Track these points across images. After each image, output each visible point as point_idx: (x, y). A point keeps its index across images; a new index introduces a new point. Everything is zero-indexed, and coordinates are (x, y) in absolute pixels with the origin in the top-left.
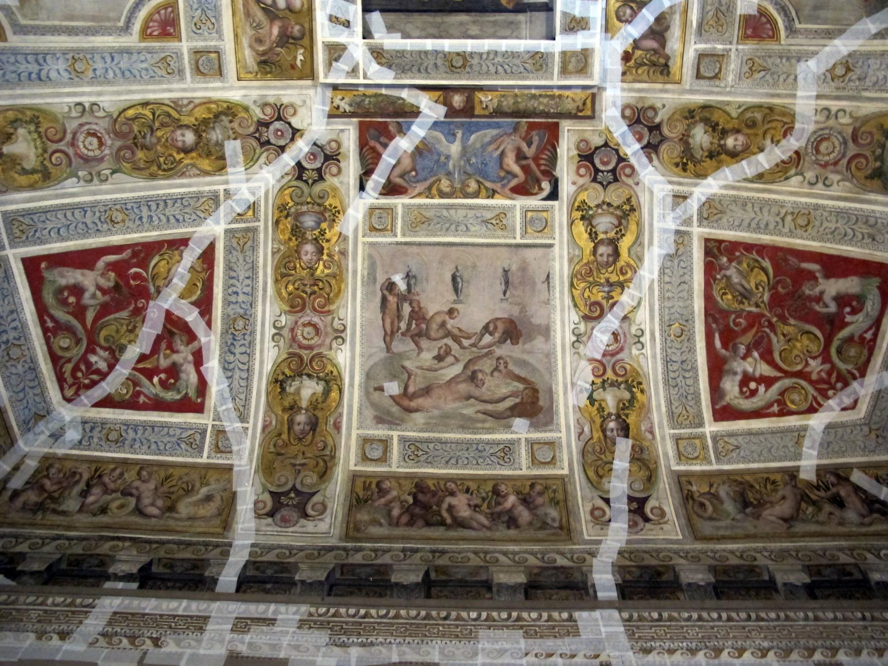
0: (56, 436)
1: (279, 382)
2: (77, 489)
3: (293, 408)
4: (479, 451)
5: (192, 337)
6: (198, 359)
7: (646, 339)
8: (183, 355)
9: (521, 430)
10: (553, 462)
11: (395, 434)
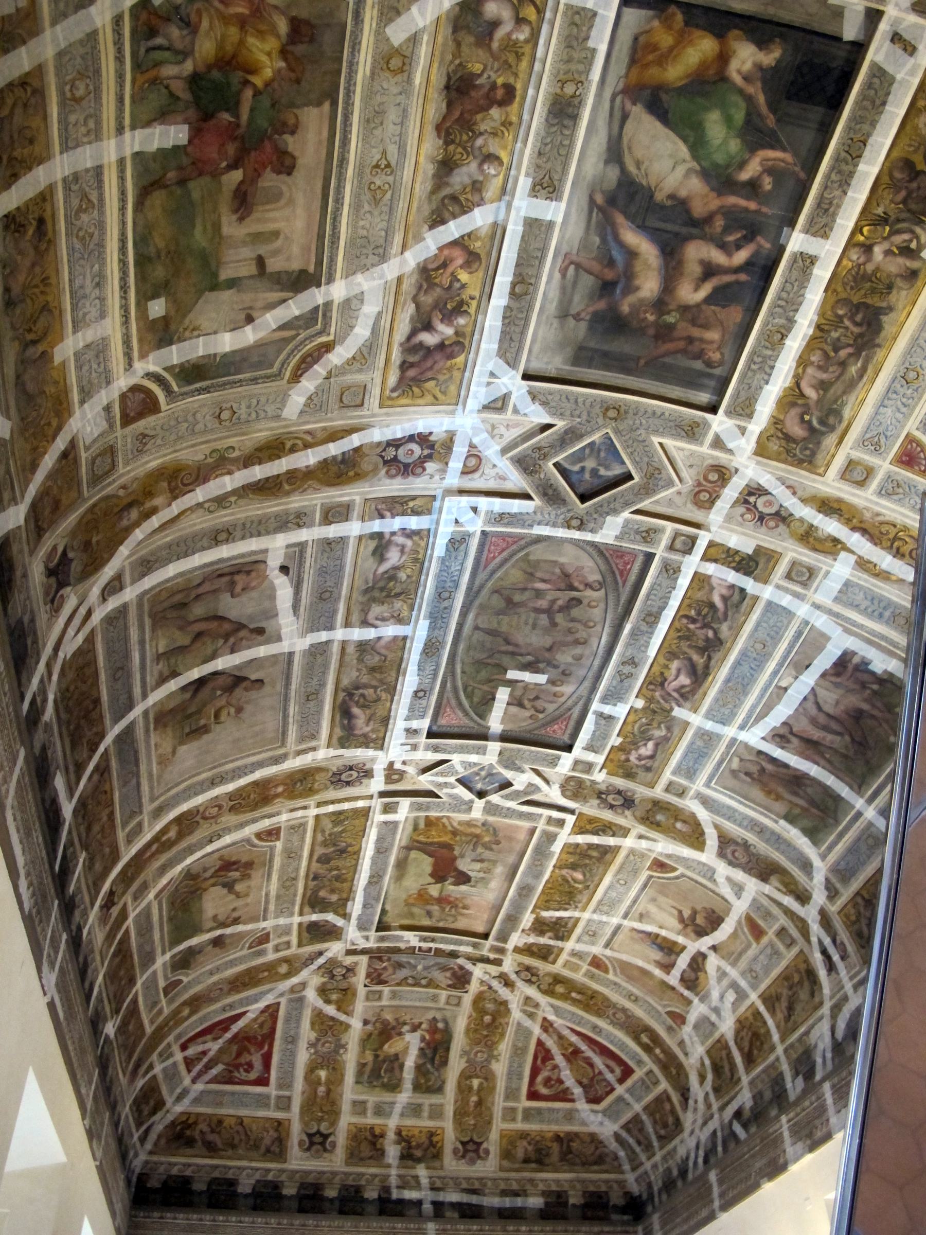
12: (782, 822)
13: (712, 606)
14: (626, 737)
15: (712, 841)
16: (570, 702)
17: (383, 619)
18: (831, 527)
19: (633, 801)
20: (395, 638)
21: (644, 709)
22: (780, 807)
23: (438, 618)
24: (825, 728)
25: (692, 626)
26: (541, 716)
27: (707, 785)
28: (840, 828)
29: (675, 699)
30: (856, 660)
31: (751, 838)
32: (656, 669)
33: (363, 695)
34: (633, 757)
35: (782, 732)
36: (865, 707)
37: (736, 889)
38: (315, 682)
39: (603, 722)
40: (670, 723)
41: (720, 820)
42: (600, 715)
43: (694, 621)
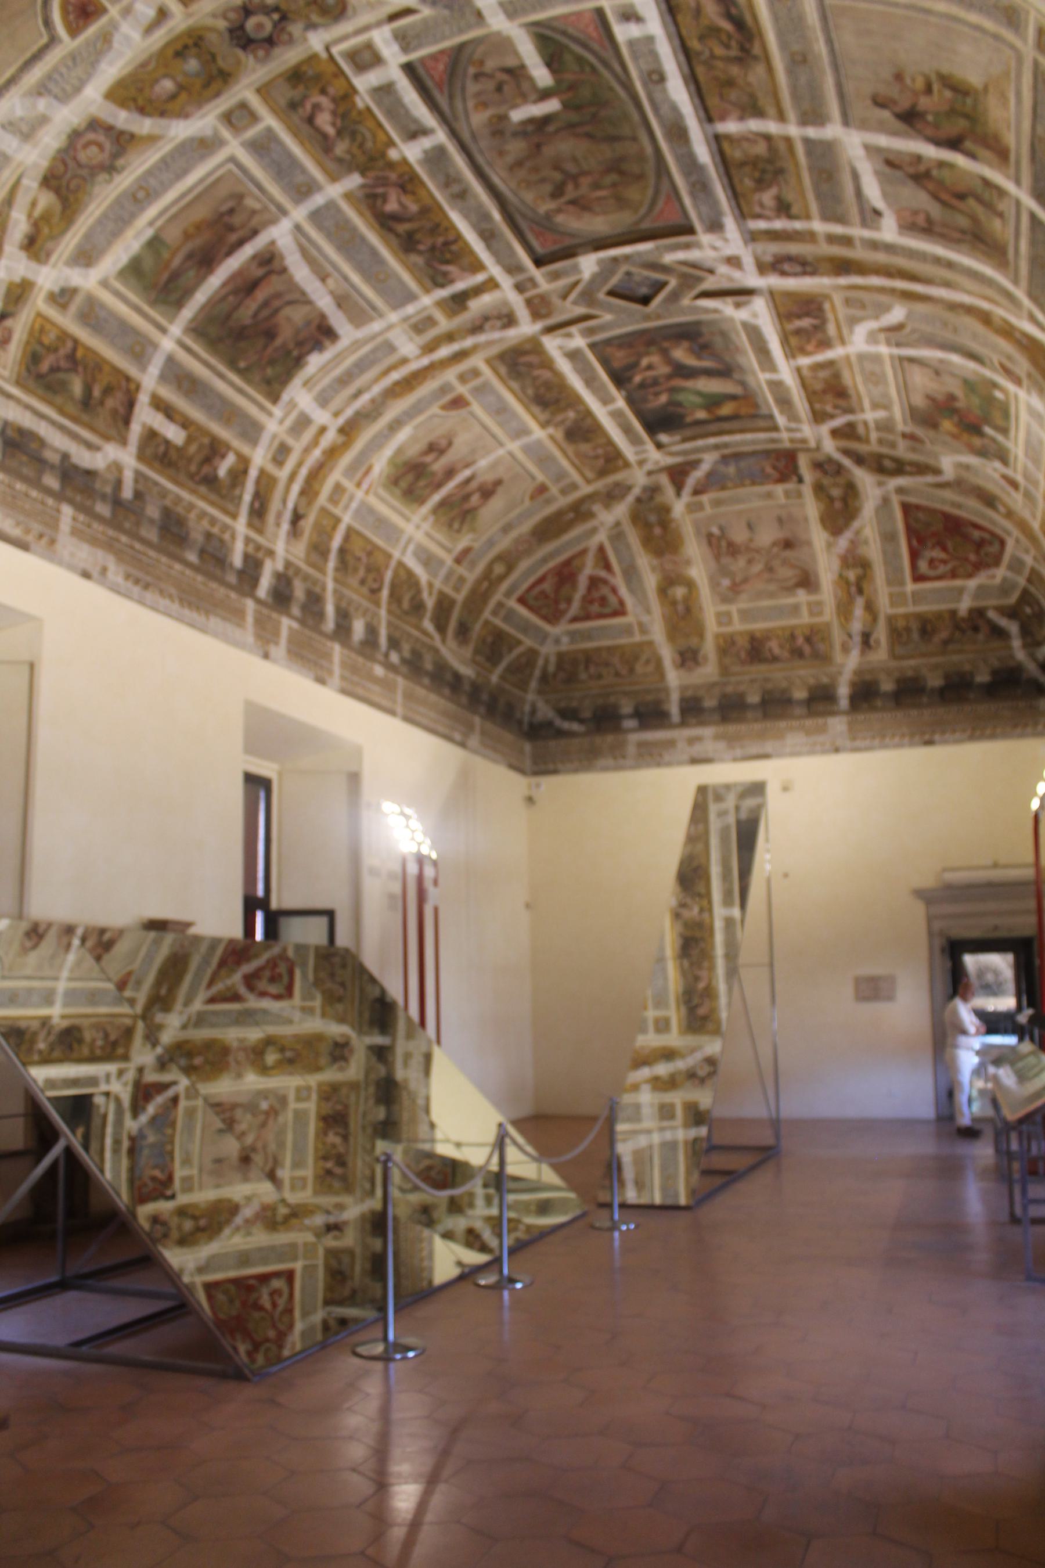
0: (557, 641)
1: (663, 591)
2: (582, 667)
3: (674, 603)
4: (780, 611)
5: (605, 582)
6: (614, 590)
7: (871, 541)
8: (605, 591)
9: (802, 596)
10: (820, 613)
11: (733, 608)
12: (150, 233)
13: (448, 262)
14: (360, 113)
15: (122, 118)
16: (459, 105)
17: (747, 139)
18: (444, 351)
19: (244, 48)
20: (723, 118)
21: (383, 155)
22: (173, 235)
23: (690, 164)
24: (266, 304)
25: (440, 240)
26: (472, 70)
27: (232, 159)
28: (146, 308)
29: (374, 186)
30: (327, 343)
31: (124, 181)
32: (422, 193)
33: (727, 47)
34: (324, 101)
35: (276, 265)
36: (278, 342)
37: (25, 128)
38: (803, 80)
39: (413, 127)
40: (347, 166)
41: (164, 149)
42: (425, 132)
43: (446, 244)
